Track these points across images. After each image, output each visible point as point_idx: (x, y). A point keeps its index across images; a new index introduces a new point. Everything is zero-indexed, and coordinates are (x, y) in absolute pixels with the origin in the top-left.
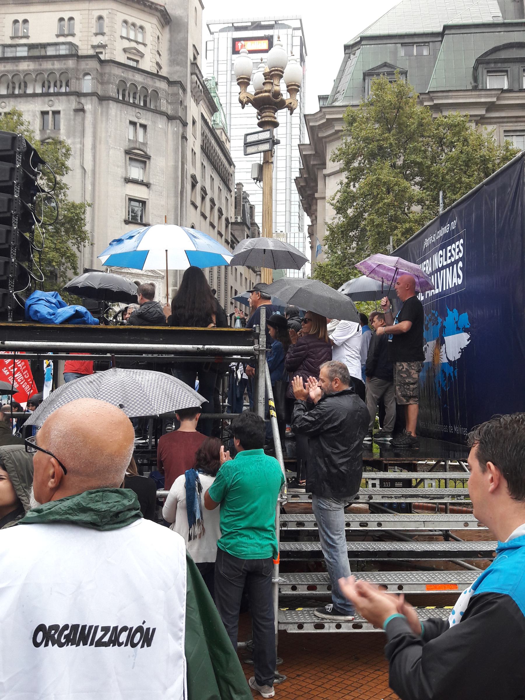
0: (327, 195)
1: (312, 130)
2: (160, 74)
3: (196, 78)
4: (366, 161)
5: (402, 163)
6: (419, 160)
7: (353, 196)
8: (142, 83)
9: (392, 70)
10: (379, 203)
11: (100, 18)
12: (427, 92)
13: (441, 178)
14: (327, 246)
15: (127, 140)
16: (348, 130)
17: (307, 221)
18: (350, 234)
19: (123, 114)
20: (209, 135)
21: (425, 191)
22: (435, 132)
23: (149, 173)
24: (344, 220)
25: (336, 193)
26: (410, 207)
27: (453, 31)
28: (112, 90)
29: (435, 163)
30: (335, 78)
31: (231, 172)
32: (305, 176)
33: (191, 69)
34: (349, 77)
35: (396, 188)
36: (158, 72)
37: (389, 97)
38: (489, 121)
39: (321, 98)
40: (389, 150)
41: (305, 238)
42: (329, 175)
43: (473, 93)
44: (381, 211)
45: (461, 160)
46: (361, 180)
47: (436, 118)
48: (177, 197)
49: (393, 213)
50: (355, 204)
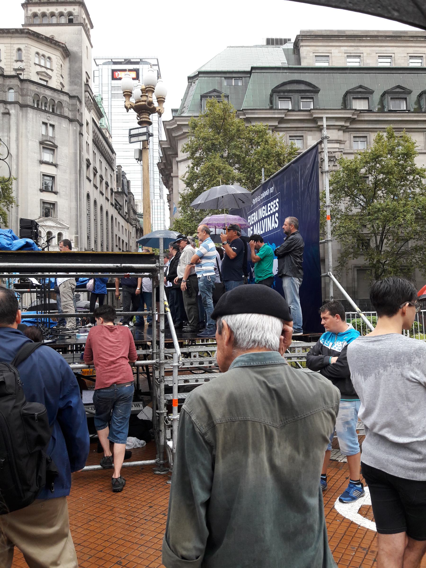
1: (168, 132)
2: (63, 90)
3: (88, 94)
6: (238, 153)
7: (197, 176)
8: (50, 96)
9: (219, 94)
10: (213, 180)
11: (19, 50)
12: (241, 109)
15: (41, 135)
16: (192, 132)
17: (166, 191)
19: (38, 117)
20: (98, 132)
21: (242, 173)
22: (247, 135)
23: (57, 157)
27: (257, 71)
28: (29, 101)
30: (182, 98)
31: (113, 158)
32: (164, 162)
33: (85, 88)
34: (191, 98)
35: (224, 171)
36: (62, 89)
37: (218, 112)
38: (280, 129)
39: (174, 111)
41: (164, 203)
42: (181, 161)
43: (270, 111)
46: (201, 165)
47: (248, 127)
48: (77, 173)
50: (198, 181)
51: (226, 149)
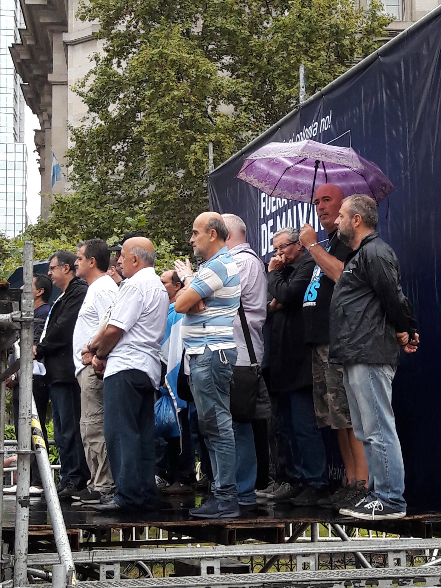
0: (69, 78)
4: (140, 24)
5: (201, 30)
6: (230, 26)
7: (119, 82)
10: (163, 96)
13: (265, 60)
14: (71, 168)
18: (113, 148)
21: (240, 80)
24: (103, 123)
25: (88, 75)
29: (256, 34)
32: (28, 43)
35: (193, 72)
40: (178, 7)
42: (75, 43)
44: (167, 109)
45: (300, 30)
46: (131, 55)
49: (189, 115)
50: (121, 96)
51: (198, 15)
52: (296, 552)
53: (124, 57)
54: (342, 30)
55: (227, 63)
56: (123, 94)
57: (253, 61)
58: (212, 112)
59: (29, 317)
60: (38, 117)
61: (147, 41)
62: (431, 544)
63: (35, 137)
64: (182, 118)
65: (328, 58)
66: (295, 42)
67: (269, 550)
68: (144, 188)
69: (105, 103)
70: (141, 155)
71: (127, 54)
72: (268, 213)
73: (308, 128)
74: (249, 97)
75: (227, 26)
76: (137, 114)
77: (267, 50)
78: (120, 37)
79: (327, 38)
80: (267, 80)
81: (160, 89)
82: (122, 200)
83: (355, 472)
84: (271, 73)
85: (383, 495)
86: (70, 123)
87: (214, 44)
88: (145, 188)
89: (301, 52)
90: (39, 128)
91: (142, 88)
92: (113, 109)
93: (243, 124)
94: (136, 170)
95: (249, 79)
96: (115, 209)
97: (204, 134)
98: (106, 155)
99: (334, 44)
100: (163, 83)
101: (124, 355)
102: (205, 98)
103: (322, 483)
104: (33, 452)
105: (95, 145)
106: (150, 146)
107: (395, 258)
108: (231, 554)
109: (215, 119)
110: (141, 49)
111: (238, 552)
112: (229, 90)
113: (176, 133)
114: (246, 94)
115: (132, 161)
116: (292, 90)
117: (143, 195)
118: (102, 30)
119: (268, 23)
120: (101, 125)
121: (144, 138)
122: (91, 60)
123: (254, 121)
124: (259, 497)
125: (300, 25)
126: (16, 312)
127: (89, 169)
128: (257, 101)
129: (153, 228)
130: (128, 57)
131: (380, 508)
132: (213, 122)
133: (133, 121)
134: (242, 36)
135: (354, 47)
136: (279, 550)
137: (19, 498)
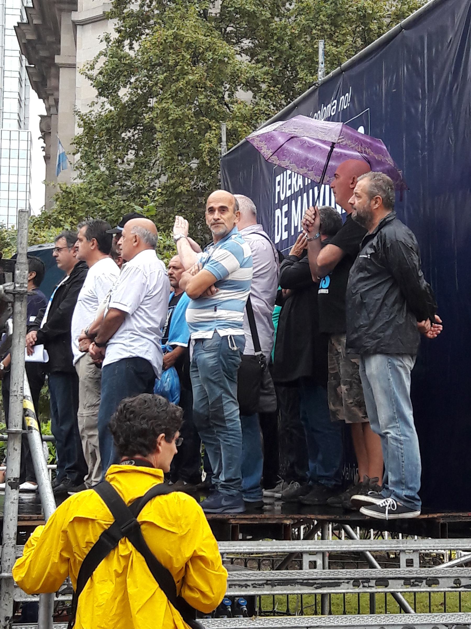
0: (78, 60)
4: (154, 3)
5: (219, 11)
7: (130, 65)
10: (178, 80)
13: (287, 44)
14: (78, 156)
18: (123, 135)
21: (260, 65)
24: (112, 108)
25: (98, 57)
26: (233, 93)
29: (278, 16)
32: (35, 22)
35: (209, 55)
42: (84, 23)
45: (324, 13)
46: (144, 36)
49: (204, 101)
50: (133, 80)
52: (303, 550)
53: (136, 39)
54: (369, 14)
55: (246, 47)
56: (135, 78)
57: (274, 45)
58: (229, 99)
59: (23, 289)
60: (44, 102)
61: (161, 21)
62: (446, 545)
63: (40, 123)
64: (197, 104)
65: (354, 43)
66: (319, 26)
67: (274, 547)
68: (155, 178)
69: (116, 87)
70: (153, 144)
71: (140, 35)
72: (282, 197)
73: (326, 107)
74: (269, 83)
75: (246, 7)
76: (149, 99)
77: (289, 33)
78: (132, 17)
79: (353, 22)
80: (289, 65)
81: (175, 72)
82: (132, 191)
83: (368, 469)
84: (293, 58)
85: (398, 491)
86: (78, 108)
87: (232, 27)
88: (156, 179)
89: (326, 37)
90: (45, 113)
91: (155, 72)
92: (124, 94)
93: (262, 112)
94: (146, 159)
95: (269, 64)
96: (124, 201)
97: (220, 121)
98: (115, 142)
99: (361, 28)
100: (178, 67)
101: (127, 342)
102: (222, 84)
103: (334, 483)
104: (24, 432)
105: (103, 132)
106: (163, 133)
107: (416, 242)
108: (233, 551)
109: (232, 106)
110: (155, 29)
111: (241, 548)
112: (248, 75)
113: (190, 120)
114: (266, 80)
115: (143, 149)
116: (315, 77)
117: (154, 186)
118: (114, 9)
119: (290, 5)
120: (111, 111)
121: (156, 125)
122: (102, 41)
123: (273, 110)
124: (266, 497)
125: (325, 7)
126: (9, 284)
127: (97, 158)
128: (278, 88)
129: (164, 221)
130: (141, 39)
131: (394, 508)
132: (229, 109)
133: (145, 107)
134: (264, 18)
135: (382, 32)
136: (285, 547)
137: (9, 480)
